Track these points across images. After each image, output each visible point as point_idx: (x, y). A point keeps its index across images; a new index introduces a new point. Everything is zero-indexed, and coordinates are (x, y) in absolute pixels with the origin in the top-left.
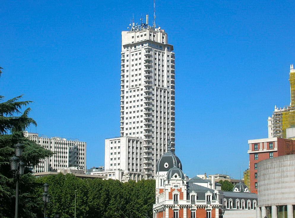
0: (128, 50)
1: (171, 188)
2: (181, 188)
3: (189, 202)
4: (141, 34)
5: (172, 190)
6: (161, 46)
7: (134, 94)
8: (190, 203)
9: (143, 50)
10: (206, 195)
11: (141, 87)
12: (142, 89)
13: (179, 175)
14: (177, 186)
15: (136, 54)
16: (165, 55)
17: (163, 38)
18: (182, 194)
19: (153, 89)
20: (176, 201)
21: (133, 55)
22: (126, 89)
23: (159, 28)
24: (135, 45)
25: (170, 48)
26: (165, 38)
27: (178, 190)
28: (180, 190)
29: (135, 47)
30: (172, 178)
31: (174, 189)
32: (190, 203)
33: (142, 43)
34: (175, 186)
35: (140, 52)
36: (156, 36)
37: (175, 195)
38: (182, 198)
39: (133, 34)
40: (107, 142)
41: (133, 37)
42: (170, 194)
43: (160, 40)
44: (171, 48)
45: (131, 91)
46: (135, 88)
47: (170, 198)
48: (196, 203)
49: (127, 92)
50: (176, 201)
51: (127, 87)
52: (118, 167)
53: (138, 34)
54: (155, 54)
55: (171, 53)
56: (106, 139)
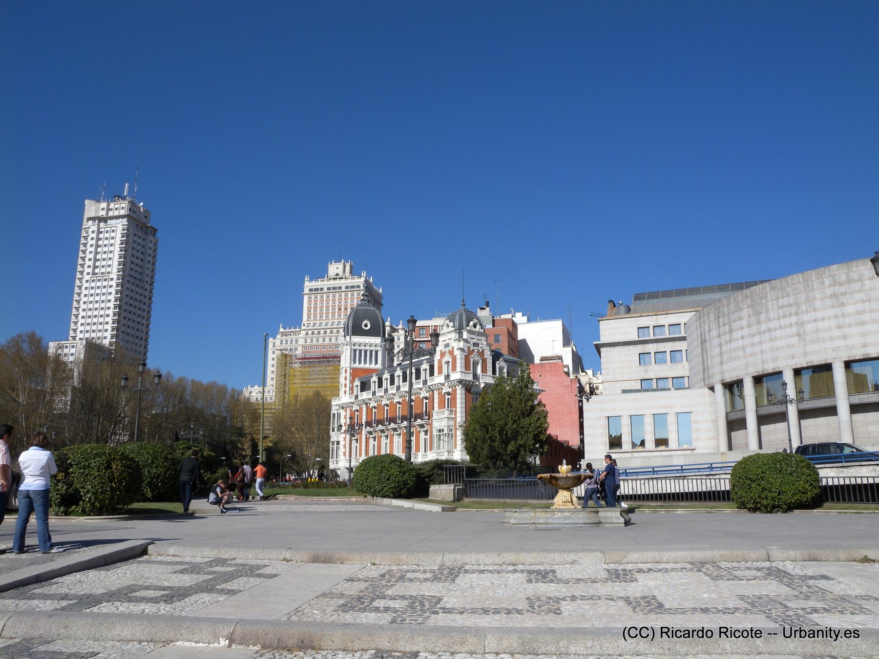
7: (99, 284)
12: (112, 279)
18: (484, 362)
29: (106, 222)
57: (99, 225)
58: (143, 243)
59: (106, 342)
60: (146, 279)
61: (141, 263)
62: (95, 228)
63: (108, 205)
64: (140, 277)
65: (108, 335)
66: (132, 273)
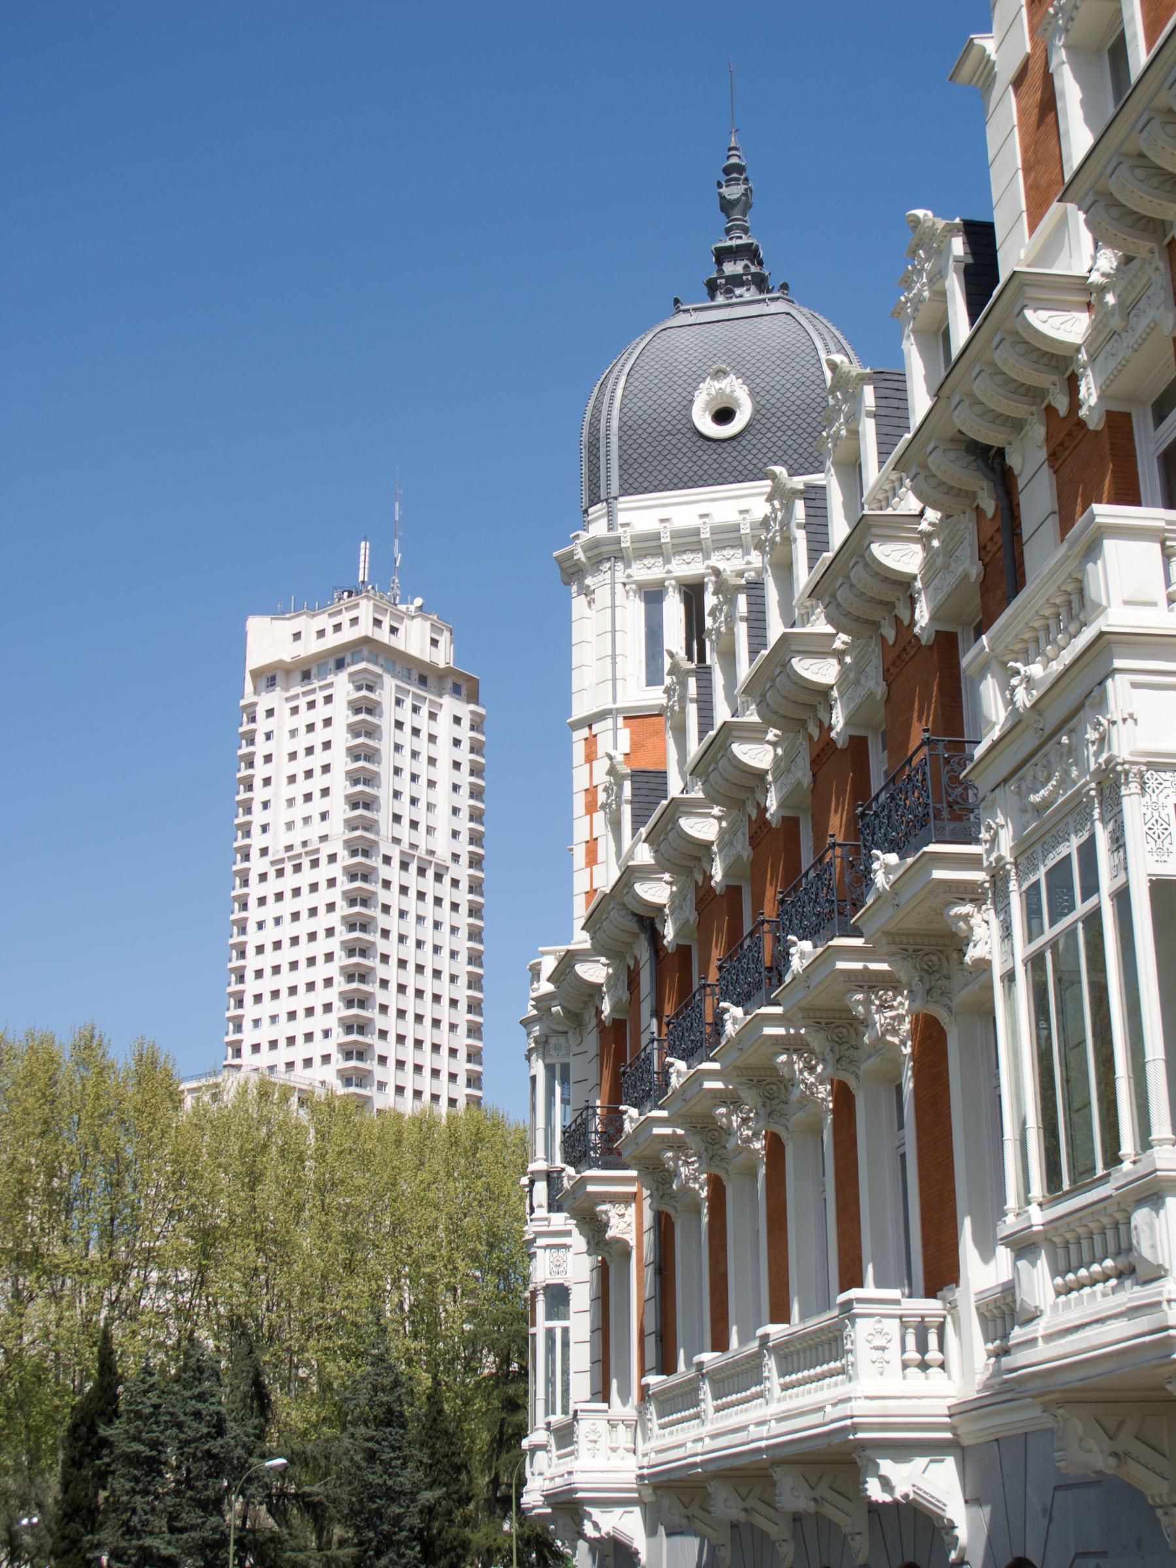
4: (336, 620)
6: (424, 676)
9: (342, 686)
11: (326, 849)
12: (332, 858)
15: (311, 705)
16: (445, 717)
17: (434, 642)
19: (387, 860)
21: (295, 710)
22: (257, 865)
23: (418, 602)
24: (304, 671)
25: (464, 691)
26: (441, 645)
33: (338, 659)
35: (327, 692)
36: (401, 633)
39: (301, 623)
41: (297, 636)
43: (422, 651)
44: (463, 685)
45: (280, 873)
46: (300, 858)
49: (263, 877)
51: (264, 852)
53: (324, 621)
54: (399, 702)
55: (472, 707)
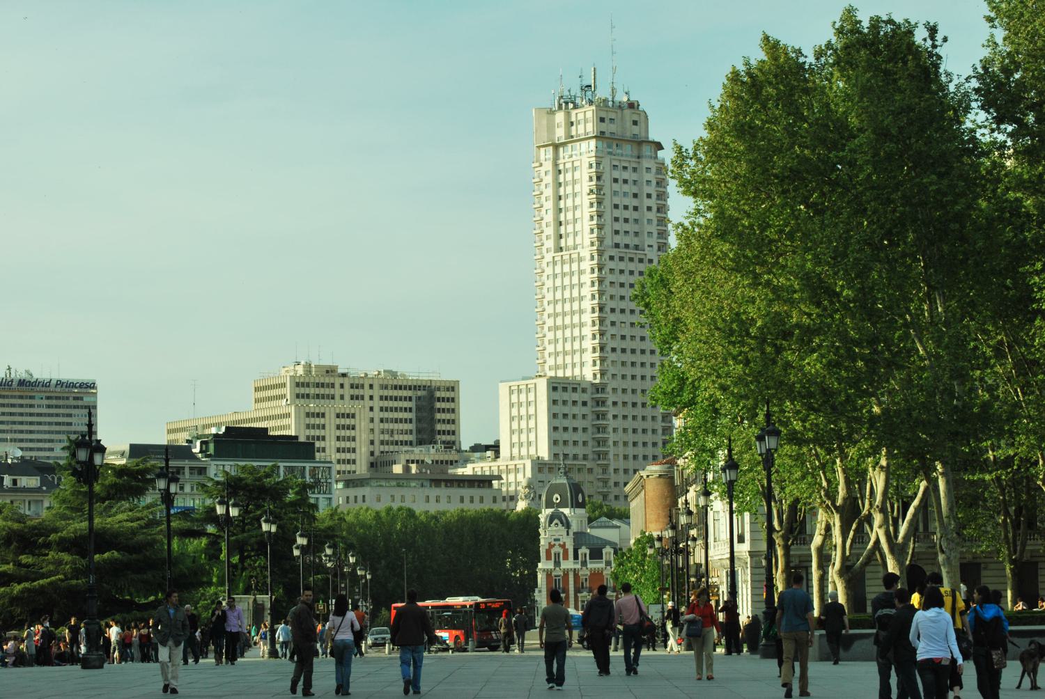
0: (549, 159)
1: (550, 543)
2: (565, 543)
3: (577, 563)
5: (551, 546)
8: (578, 566)
10: (604, 552)
13: (562, 523)
14: (559, 540)
18: (566, 552)
20: (557, 563)
27: (560, 545)
28: (563, 546)
30: (550, 529)
31: (555, 545)
32: (578, 566)
34: (555, 540)
37: (555, 554)
38: (566, 558)
40: (503, 389)
42: (548, 552)
47: (548, 558)
48: (589, 566)
50: (557, 563)
52: (532, 451)
56: (501, 382)
57: (556, 158)
58: (634, 176)
59: (589, 372)
60: (648, 241)
61: (635, 215)
62: (548, 166)
63: (568, 114)
64: (636, 241)
65: (589, 357)
66: (618, 239)
